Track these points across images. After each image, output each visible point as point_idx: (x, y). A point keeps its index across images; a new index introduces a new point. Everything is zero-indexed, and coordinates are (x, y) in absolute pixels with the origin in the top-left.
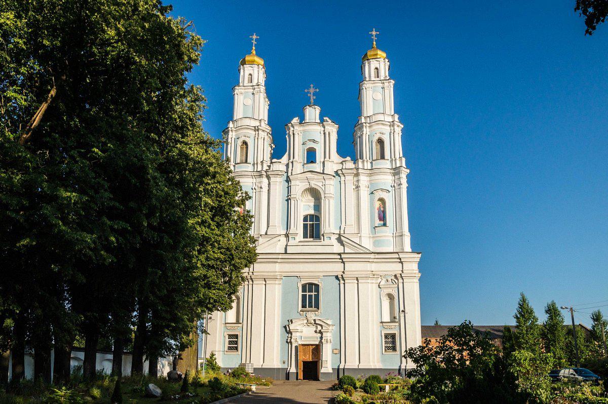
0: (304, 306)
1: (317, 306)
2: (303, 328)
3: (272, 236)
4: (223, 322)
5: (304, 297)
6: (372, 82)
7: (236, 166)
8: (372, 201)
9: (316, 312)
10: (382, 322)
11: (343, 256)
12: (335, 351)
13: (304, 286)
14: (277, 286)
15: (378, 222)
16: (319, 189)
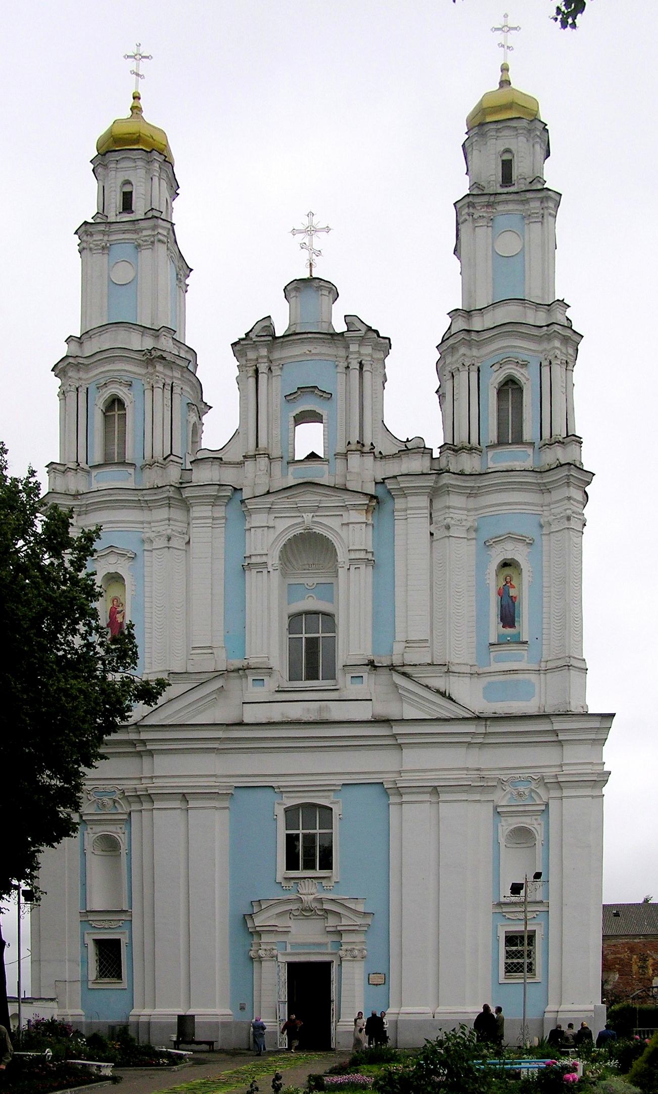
0: (292, 864)
1: (327, 864)
2: (290, 923)
3: (198, 676)
4: (78, 908)
5: (291, 840)
6: (492, 199)
7: (94, 473)
8: (481, 567)
9: (324, 882)
10: (500, 904)
11: (397, 729)
12: (375, 979)
13: (290, 812)
14: (218, 815)
15: (494, 629)
16: (330, 536)
